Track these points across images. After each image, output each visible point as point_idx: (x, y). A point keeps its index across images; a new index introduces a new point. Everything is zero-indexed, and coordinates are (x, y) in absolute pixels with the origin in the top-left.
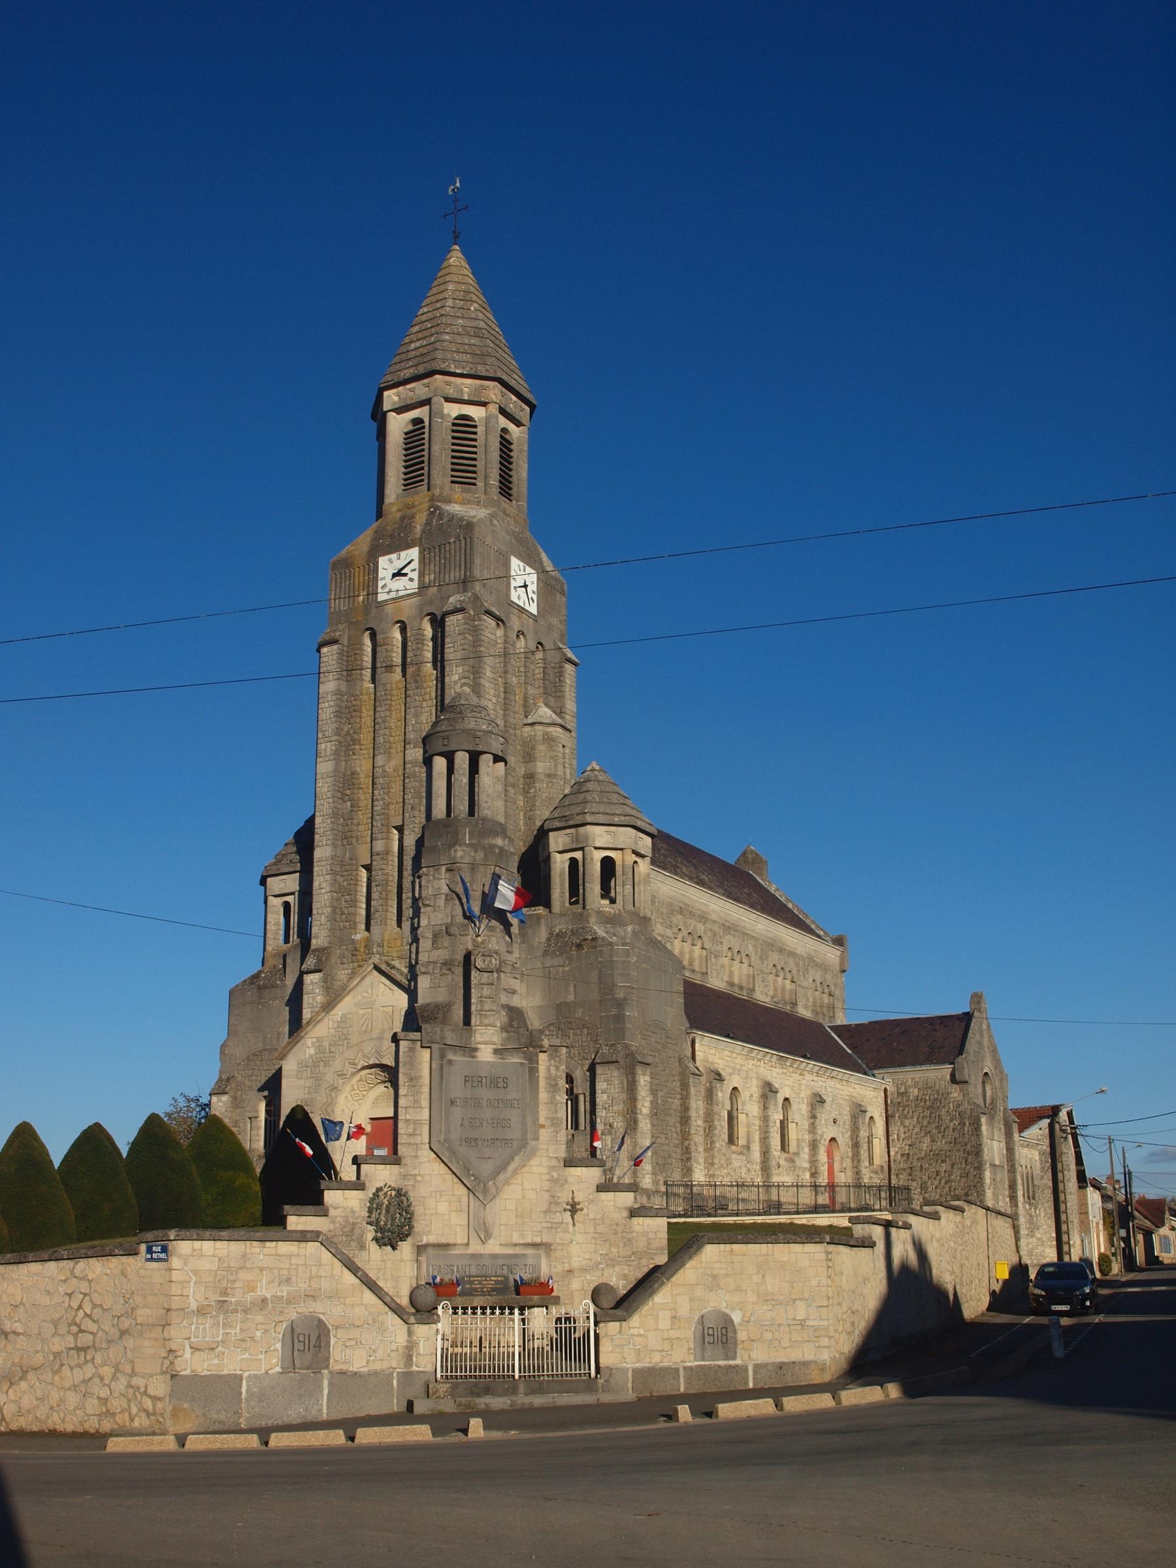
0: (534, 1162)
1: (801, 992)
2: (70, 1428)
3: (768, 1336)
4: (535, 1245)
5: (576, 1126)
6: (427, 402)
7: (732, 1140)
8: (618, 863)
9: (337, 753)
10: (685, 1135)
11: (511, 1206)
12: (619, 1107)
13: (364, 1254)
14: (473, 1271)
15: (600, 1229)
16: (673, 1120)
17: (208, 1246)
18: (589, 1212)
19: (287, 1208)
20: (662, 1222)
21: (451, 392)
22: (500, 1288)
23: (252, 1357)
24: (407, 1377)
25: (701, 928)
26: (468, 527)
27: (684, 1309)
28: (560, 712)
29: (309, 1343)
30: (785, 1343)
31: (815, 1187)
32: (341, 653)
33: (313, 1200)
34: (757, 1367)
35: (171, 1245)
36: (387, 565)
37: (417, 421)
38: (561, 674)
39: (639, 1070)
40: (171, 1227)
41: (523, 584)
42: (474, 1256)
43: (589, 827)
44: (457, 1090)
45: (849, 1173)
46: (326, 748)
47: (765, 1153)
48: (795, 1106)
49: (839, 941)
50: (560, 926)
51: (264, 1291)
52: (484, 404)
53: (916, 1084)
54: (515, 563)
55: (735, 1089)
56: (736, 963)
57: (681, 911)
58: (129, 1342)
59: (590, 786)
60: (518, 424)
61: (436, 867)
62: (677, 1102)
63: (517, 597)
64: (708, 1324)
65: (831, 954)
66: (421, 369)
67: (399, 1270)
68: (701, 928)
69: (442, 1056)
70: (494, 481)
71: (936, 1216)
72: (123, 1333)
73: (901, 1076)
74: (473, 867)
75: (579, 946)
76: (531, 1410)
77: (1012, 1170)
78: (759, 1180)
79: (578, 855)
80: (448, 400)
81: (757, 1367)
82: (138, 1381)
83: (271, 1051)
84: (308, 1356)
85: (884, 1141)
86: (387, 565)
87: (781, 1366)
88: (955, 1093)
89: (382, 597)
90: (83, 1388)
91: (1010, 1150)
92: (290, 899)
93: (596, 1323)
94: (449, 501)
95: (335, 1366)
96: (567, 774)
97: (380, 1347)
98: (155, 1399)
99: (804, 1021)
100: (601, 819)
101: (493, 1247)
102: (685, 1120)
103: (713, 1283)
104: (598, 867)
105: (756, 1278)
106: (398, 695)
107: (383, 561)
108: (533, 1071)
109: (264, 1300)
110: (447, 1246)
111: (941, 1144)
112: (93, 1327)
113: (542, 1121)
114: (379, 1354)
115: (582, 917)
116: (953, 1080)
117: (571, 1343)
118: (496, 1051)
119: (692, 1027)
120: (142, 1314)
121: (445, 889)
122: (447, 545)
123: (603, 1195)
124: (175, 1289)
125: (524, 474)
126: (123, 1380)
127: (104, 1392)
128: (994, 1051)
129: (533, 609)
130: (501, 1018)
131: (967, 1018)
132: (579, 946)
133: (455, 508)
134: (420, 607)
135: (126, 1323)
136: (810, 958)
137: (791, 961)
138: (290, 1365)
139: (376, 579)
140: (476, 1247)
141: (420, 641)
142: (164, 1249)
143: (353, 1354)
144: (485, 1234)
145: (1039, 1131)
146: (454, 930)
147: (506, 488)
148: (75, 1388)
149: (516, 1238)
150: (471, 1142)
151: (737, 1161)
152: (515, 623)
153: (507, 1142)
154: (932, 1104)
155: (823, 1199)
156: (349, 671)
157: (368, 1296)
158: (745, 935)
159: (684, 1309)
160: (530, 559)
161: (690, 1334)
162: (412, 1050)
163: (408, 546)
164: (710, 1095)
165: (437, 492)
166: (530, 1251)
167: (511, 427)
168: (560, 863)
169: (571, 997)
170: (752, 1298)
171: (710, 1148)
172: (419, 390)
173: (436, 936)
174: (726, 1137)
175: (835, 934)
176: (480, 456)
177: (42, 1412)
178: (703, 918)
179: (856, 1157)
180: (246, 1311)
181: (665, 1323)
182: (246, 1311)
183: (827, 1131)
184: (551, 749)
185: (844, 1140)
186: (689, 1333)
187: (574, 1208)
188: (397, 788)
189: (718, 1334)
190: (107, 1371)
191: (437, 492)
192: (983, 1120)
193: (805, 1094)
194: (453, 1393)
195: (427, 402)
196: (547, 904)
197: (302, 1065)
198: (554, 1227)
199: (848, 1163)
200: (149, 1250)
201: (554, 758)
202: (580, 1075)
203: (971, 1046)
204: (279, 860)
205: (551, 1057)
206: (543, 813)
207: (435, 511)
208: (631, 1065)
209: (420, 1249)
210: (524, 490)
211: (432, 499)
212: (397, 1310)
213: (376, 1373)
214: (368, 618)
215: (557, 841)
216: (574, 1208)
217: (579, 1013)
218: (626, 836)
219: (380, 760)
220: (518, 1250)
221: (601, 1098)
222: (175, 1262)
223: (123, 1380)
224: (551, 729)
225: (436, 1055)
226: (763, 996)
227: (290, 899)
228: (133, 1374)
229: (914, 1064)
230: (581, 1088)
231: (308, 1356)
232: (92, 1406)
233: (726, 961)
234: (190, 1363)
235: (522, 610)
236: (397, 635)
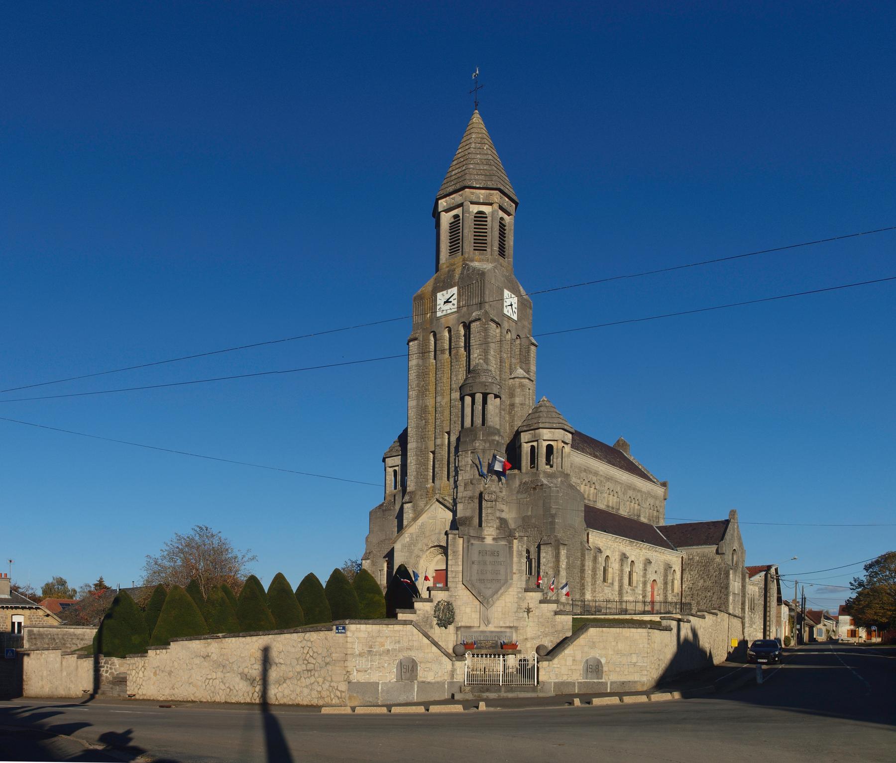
1: (643, 510)
3: (618, 669)
4: (510, 627)
5: (530, 573)
8: (555, 447)
11: (500, 609)
13: (432, 630)
14: (482, 638)
18: (535, 612)
19: (398, 610)
20: (570, 617)
22: (494, 646)
24: (451, 684)
27: (579, 656)
29: (408, 669)
30: (626, 673)
33: (410, 607)
34: (612, 683)
39: (561, 547)
42: (482, 632)
44: (475, 557)
49: (664, 485)
50: (526, 479)
53: (698, 554)
56: (611, 496)
57: (585, 471)
59: (542, 409)
61: (466, 451)
65: (660, 491)
67: (448, 637)
68: (594, 479)
69: (468, 542)
71: (703, 617)
74: (484, 451)
75: (535, 489)
76: (507, 699)
77: (744, 596)
79: (535, 444)
81: (612, 683)
84: (408, 675)
87: (623, 683)
88: (718, 559)
91: (744, 587)
93: (538, 662)
95: (420, 679)
96: (531, 403)
97: (440, 671)
100: (547, 425)
101: (491, 628)
103: (593, 645)
105: (613, 644)
108: (511, 548)
111: (709, 583)
113: (514, 571)
114: (440, 674)
115: (536, 475)
116: (717, 552)
117: (525, 670)
118: (494, 539)
119: (588, 527)
121: (470, 462)
123: (542, 605)
130: (496, 523)
136: (649, 493)
137: (639, 494)
138: (400, 678)
140: (483, 628)
141: (458, 337)
145: (759, 577)
146: (474, 482)
149: (502, 624)
150: (481, 581)
153: (498, 580)
154: (705, 564)
156: (423, 353)
157: (434, 649)
158: (616, 482)
159: (579, 656)
162: (454, 538)
166: (508, 630)
168: (526, 448)
169: (530, 513)
170: (611, 652)
175: (662, 481)
178: (596, 474)
181: (569, 662)
184: (523, 390)
186: (581, 667)
187: (528, 611)
189: (594, 668)
192: (731, 572)
194: (472, 691)
196: (520, 469)
201: (524, 395)
202: (533, 550)
203: (728, 536)
205: (519, 541)
206: (518, 423)
208: (557, 545)
209: (458, 629)
212: (447, 655)
213: (438, 682)
214: (432, 327)
215: (525, 437)
216: (528, 611)
217: (533, 521)
220: (503, 630)
221: (543, 560)
225: (466, 541)
226: (624, 512)
229: (698, 545)
230: (533, 556)
231: (408, 675)
233: (606, 495)
236: (447, 334)
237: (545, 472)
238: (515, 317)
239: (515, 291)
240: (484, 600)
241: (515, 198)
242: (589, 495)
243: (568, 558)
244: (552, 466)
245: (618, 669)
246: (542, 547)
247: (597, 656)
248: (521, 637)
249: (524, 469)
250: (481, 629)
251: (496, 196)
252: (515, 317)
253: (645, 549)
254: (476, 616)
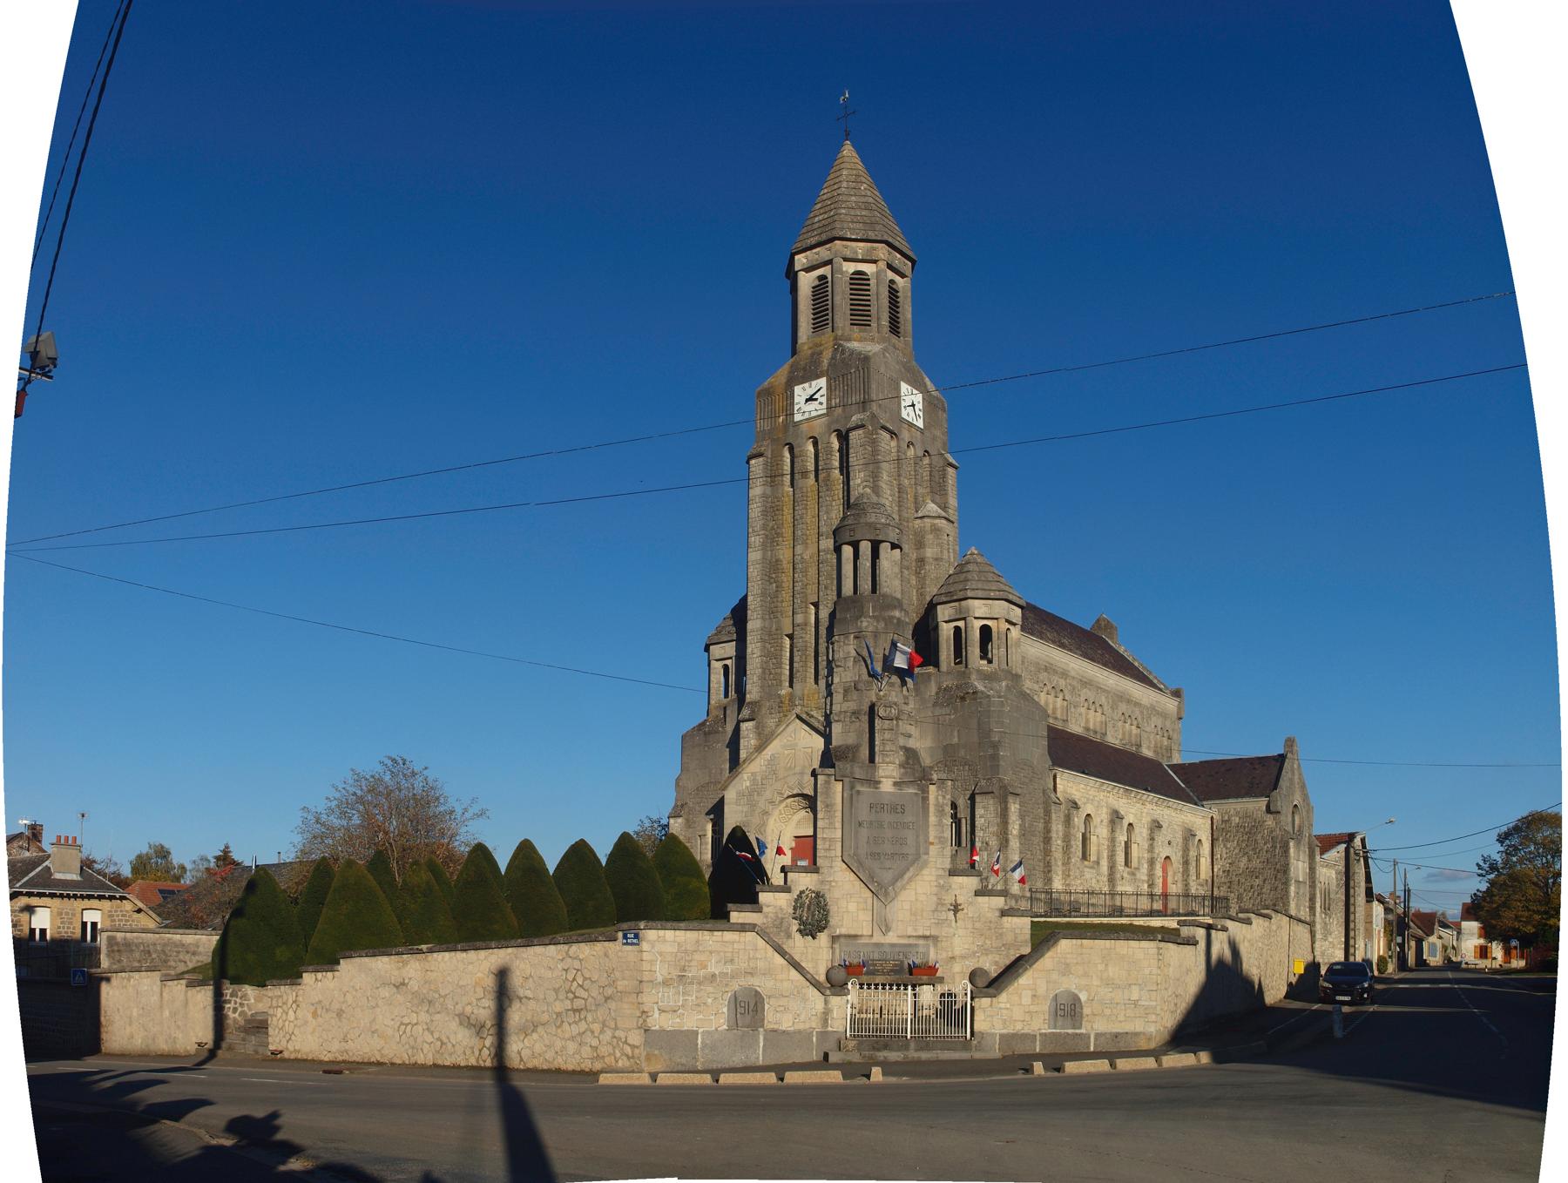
0: (925, 872)
1: (1145, 735)
2: (570, 1067)
3: (1108, 1012)
4: (925, 937)
5: (959, 843)
6: (829, 262)
7: (1085, 857)
8: (994, 630)
9: (764, 545)
10: (1047, 852)
11: (907, 906)
12: (994, 829)
13: (790, 942)
14: (876, 956)
15: (977, 925)
16: (1037, 840)
17: (669, 934)
18: (968, 911)
21: (848, 254)
22: (897, 970)
23: (708, 1018)
24: (823, 1035)
25: (1062, 683)
26: (865, 359)
27: (1042, 989)
28: (944, 508)
29: (748, 1008)
30: (1121, 1018)
31: (1151, 895)
32: (765, 464)
33: (751, 900)
34: (1097, 1035)
35: (642, 933)
36: (801, 392)
37: (822, 278)
38: (944, 476)
39: (1011, 799)
40: (641, 919)
41: (911, 403)
42: (877, 945)
43: (970, 601)
44: (864, 814)
45: (1180, 885)
46: (755, 540)
47: (1112, 867)
48: (1137, 829)
49: (1177, 694)
51: (714, 968)
52: (875, 262)
54: (905, 387)
57: (1046, 669)
58: (612, 1005)
59: (970, 567)
60: (903, 276)
61: (846, 635)
62: (1041, 825)
63: (907, 414)
64: (1060, 1001)
65: (1171, 705)
66: (824, 237)
67: (818, 954)
68: (1062, 683)
69: (852, 788)
70: (885, 322)
72: (607, 999)
73: (1225, 807)
74: (876, 635)
75: (963, 699)
76: (919, 1062)
78: (1106, 889)
79: (961, 624)
80: (846, 260)
81: (1097, 1035)
82: (617, 1033)
83: (716, 783)
84: (748, 1018)
86: (801, 392)
88: (1270, 821)
89: (798, 417)
90: (579, 1038)
92: (728, 662)
94: (849, 340)
95: (768, 1026)
96: (951, 558)
97: (803, 1012)
98: (633, 1047)
99: (1147, 759)
100: (980, 594)
101: (891, 938)
102: (1047, 840)
103: (1066, 970)
105: (1100, 967)
106: (813, 496)
107: (798, 389)
108: (925, 799)
109: (714, 976)
110: (856, 936)
111: (1256, 863)
112: (584, 994)
114: (803, 1017)
115: (965, 675)
116: (1268, 810)
117: (952, 1013)
118: (895, 784)
120: (621, 984)
121: (853, 653)
122: (850, 376)
123: (980, 899)
124: (646, 966)
125: (909, 316)
126: (609, 1033)
127: (595, 1043)
128: (1303, 787)
129: (920, 423)
130: (899, 757)
131: (1281, 759)
132: (963, 699)
133: (855, 345)
134: (829, 426)
135: (609, 991)
136: (1153, 708)
137: (1137, 711)
138: (734, 1024)
139: (792, 404)
140: (878, 938)
141: (829, 452)
142: (636, 936)
143: (779, 1017)
144: (886, 928)
147: (895, 327)
148: (573, 1038)
149: (910, 932)
150: (875, 856)
151: (1089, 874)
152: (906, 436)
153: (904, 856)
154: (1250, 830)
155: (1158, 906)
156: (773, 477)
157: (794, 973)
158: (1099, 689)
159: (1042, 989)
160: (917, 384)
161: (1046, 1008)
162: (827, 782)
163: (818, 377)
164: (1068, 820)
165: (840, 333)
166: (921, 942)
167: (897, 279)
168: (946, 630)
169: (956, 740)
170: (1096, 982)
171: (1066, 863)
172: (823, 253)
173: (846, 691)
174: (1080, 854)
175: (1174, 687)
176: (873, 303)
177: (549, 1055)
178: (1064, 674)
179: (1186, 872)
180: (700, 983)
181: (1026, 1000)
182: (700, 983)
183: (1162, 851)
185: (1176, 858)
186: (1045, 1007)
187: (956, 908)
188: (813, 571)
189: (1068, 1009)
190: (596, 1027)
191: (840, 333)
193: (1146, 820)
194: (859, 1048)
195: (829, 262)
196: (937, 665)
197: (740, 794)
198: (939, 923)
199: (1179, 877)
200: (625, 937)
202: (962, 803)
203: (1284, 783)
204: (719, 631)
205: (939, 788)
206: (932, 590)
207: (838, 348)
208: (1004, 795)
209: (834, 939)
210: (910, 328)
211: (836, 339)
212: (816, 984)
213: (800, 1032)
214: (787, 436)
215: (943, 612)
216: (956, 908)
217: (962, 753)
218: (1000, 608)
219: (799, 549)
220: (912, 941)
221: (979, 822)
222: (645, 946)
223: (609, 1033)
224: (937, 521)
226: (1113, 739)
227: (728, 662)
228: (616, 1028)
229: (1237, 796)
230: (963, 813)
231: (748, 1018)
232: (586, 1052)
233: (1083, 710)
234: (658, 1021)
235: (911, 425)
236: (811, 448)
237: (979, 671)
240: (880, 890)
242: (1055, 709)
243: (1022, 817)
244: (990, 662)
245: (1108, 1012)
246: (978, 799)
247: (1073, 989)
248: (944, 955)
249: (944, 666)
250: (874, 940)
254: (865, 917)
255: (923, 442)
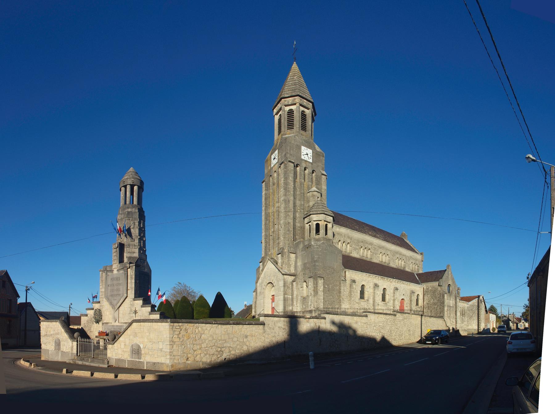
25: (370, 247)
38: (321, 178)
55: (384, 289)
57: (362, 242)
77: (456, 308)
85: (422, 300)
88: (439, 288)
99: (407, 272)
104: (315, 226)
111: (436, 301)
154: (434, 291)
192: (446, 295)
237: (314, 238)
238: (311, 161)
239: (309, 146)
241: (312, 100)
251: (297, 99)
252: (311, 161)
253: (395, 282)
255: (312, 167)
